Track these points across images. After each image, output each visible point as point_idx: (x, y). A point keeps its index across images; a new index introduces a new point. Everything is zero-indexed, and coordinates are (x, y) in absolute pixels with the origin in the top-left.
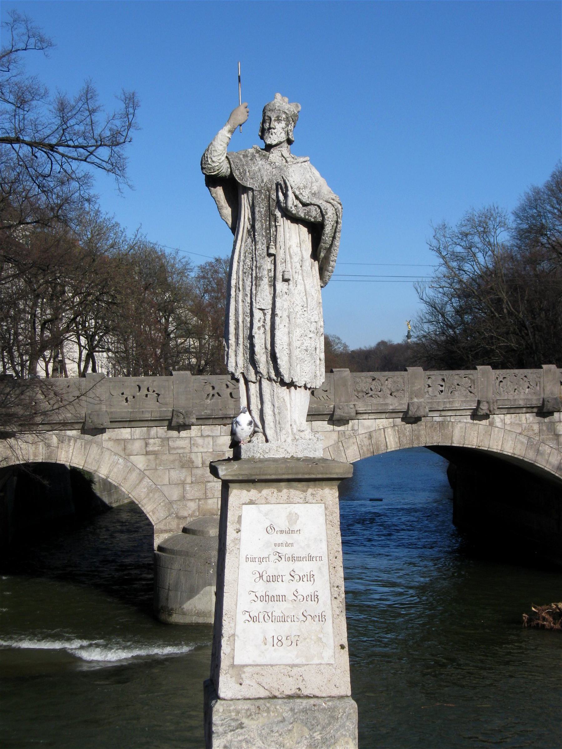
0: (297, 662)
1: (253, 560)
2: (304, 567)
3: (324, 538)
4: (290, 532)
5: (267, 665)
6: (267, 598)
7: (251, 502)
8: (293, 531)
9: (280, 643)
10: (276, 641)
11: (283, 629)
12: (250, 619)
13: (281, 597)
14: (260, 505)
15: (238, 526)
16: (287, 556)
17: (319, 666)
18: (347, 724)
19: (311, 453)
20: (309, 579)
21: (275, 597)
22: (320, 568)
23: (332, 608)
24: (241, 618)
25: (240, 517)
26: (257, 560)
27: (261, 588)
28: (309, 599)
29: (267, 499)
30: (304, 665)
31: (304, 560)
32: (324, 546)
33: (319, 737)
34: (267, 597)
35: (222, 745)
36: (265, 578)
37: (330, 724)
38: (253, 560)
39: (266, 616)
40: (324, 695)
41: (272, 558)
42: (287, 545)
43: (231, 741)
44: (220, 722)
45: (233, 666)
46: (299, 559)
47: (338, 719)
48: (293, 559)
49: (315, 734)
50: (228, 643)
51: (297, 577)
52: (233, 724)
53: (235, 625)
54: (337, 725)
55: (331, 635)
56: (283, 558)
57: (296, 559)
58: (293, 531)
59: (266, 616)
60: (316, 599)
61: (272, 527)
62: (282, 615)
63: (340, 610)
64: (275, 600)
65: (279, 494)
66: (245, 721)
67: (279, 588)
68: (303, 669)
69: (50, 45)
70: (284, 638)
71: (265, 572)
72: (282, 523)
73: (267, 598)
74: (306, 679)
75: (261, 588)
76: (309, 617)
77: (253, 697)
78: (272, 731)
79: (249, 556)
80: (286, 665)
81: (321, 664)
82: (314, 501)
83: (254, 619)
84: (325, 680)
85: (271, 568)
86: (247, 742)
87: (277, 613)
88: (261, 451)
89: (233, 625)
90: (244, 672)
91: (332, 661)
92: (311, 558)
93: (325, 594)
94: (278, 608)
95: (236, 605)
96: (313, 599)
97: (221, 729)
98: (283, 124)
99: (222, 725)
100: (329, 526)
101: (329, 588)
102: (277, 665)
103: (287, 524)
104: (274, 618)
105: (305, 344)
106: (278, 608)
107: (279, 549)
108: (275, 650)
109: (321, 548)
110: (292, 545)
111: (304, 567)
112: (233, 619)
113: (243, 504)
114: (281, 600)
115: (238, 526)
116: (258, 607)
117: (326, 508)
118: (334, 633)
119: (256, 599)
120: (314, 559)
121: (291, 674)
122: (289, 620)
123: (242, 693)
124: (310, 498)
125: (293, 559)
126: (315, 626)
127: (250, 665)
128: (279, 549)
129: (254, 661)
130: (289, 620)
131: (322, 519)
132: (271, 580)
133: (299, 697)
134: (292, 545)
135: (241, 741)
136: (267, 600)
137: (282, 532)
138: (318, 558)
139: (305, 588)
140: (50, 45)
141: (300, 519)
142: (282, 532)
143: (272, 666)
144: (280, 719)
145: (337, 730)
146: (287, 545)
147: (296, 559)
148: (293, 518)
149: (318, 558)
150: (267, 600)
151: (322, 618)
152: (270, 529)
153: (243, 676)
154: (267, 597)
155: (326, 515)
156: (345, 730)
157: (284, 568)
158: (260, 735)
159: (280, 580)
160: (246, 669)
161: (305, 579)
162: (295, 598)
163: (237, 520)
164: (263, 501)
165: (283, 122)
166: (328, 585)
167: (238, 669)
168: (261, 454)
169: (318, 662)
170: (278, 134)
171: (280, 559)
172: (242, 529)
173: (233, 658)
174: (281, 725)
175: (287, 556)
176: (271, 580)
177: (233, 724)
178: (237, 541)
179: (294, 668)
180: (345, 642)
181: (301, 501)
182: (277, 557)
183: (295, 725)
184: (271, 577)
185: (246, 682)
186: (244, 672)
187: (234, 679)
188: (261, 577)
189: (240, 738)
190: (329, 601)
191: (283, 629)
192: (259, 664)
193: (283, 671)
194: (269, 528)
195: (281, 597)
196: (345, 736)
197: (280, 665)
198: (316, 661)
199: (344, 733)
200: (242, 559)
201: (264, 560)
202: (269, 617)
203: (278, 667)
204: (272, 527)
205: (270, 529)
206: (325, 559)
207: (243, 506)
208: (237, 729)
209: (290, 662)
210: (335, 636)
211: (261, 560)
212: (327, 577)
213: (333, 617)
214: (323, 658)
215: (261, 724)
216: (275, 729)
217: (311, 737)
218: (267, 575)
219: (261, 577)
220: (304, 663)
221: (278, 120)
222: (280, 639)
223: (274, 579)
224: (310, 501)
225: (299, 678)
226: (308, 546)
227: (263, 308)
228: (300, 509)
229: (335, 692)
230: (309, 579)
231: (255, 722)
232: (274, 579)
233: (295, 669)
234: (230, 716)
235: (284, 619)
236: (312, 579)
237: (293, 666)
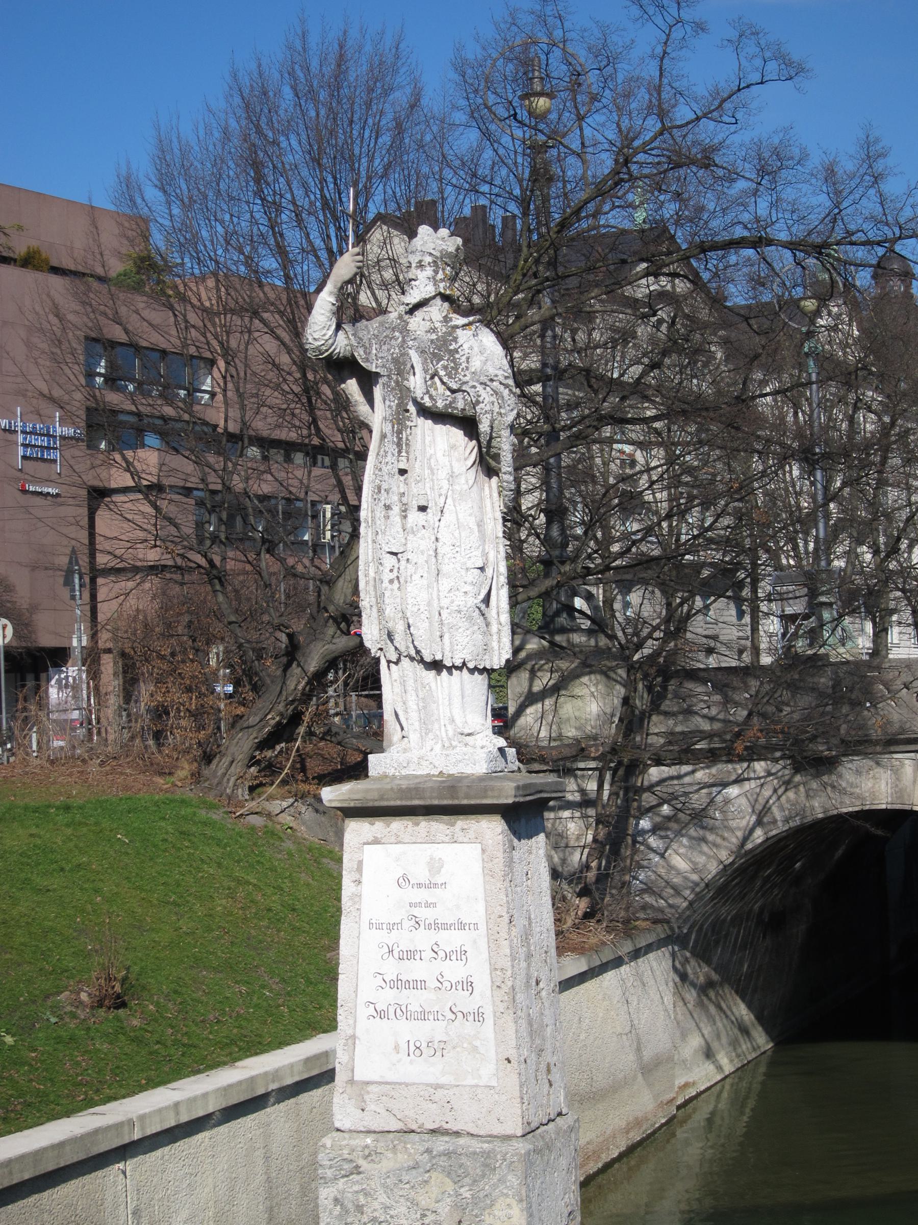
0: (443, 1080)
1: (379, 927)
2: (451, 940)
3: (480, 894)
4: (432, 885)
5: (400, 1084)
6: (398, 984)
7: (376, 841)
9: (418, 1052)
10: (412, 1048)
11: (422, 1031)
15: (358, 876)
18: (509, 1178)
22: (475, 942)
23: (494, 1002)
24: (364, 1012)
25: (360, 863)
27: (391, 969)
28: (460, 987)
29: (398, 836)
32: (481, 907)
33: (468, 1195)
35: (332, 1195)
36: (396, 953)
37: (483, 1176)
38: (379, 927)
39: (398, 1011)
41: (407, 924)
42: (428, 905)
43: (344, 1192)
44: (328, 1163)
45: (351, 1082)
46: (446, 927)
47: (495, 1169)
48: (437, 926)
49: (462, 1190)
52: (346, 1166)
54: (495, 1179)
56: (422, 924)
59: (398, 1011)
61: (405, 877)
63: (505, 1004)
65: (416, 828)
66: (361, 1162)
67: (416, 970)
68: (451, 1092)
69: (801, 70)
70: (424, 1045)
72: (421, 874)
73: (398, 984)
74: (455, 1107)
75: (391, 969)
76: (460, 1015)
77: (381, 1129)
78: (400, 1181)
80: (427, 1085)
81: (477, 1086)
82: (465, 840)
83: (381, 1014)
84: (484, 1110)
85: (405, 939)
86: (366, 1194)
87: (414, 1007)
88: (395, 765)
89: (351, 1022)
90: (368, 1093)
91: (494, 1083)
92: (462, 926)
93: (483, 981)
94: (415, 1000)
95: (356, 992)
97: (329, 1173)
98: (429, 271)
99: (331, 1167)
100: (488, 878)
103: (427, 873)
105: (457, 603)
106: (415, 1000)
107: (416, 911)
108: (411, 1062)
111: (451, 940)
112: (353, 1014)
113: (365, 844)
115: (358, 876)
116: (385, 998)
117: (483, 851)
118: (496, 1038)
119: (384, 985)
121: (435, 1098)
122: (431, 1017)
124: (459, 835)
125: (437, 926)
126: (469, 1027)
127: (376, 1083)
128: (416, 911)
130: (431, 1017)
131: (477, 867)
135: (357, 1192)
137: (419, 885)
139: (454, 971)
140: (801, 70)
142: (419, 885)
143: (407, 1085)
144: (411, 1163)
145: (495, 1186)
146: (428, 905)
148: (435, 866)
151: (479, 1016)
152: (404, 880)
153: (366, 1097)
156: (507, 1187)
157: (423, 940)
158: (384, 1186)
159: (417, 957)
160: (371, 1088)
161: (453, 957)
162: (439, 985)
164: (393, 839)
165: (428, 268)
166: (487, 967)
167: (360, 1087)
170: (422, 286)
172: (364, 879)
173: (353, 1071)
174: (414, 1172)
177: (346, 1166)
178: (357, 897)
180: (512, 1053)
181: (447, 839)
182: (413, 922)
183: (434, 1175)
185: (371, 1107)
186: (368, 1093)
187: (353, 1101)
188: (391, 951)
189: (356, 1188)
190: (489, 993)
191: (422, 1031)
193: (422, 1093)
194: (401, 880)
196: (507, 1195)
198: (470, 1081)
199: (505, 1191)
200: (365, 925)
202: (403, 1012)
204: (405, 877)
205: (404, 880)
206: (483, 927)
208: (352, 1174)
209: (432, 1080)
211: (391, 927)
212: (485, 955)
214: (480, 1077)
215: (385, 1170)
216: (405, 1178)
217: (458, 1195)
219: (391, 951)
220: (453, 1083)
221: (420, 265)
223: (410, 955)
224: (460, 839)
227: (395, 551)
228: (444, 851)
229: (498, 1130)
231: (376, 1166)
232: (410, 955)
233: (440, 1093)
234: (340, 1155)
235: (423, 1016)
237: (437, 1087)
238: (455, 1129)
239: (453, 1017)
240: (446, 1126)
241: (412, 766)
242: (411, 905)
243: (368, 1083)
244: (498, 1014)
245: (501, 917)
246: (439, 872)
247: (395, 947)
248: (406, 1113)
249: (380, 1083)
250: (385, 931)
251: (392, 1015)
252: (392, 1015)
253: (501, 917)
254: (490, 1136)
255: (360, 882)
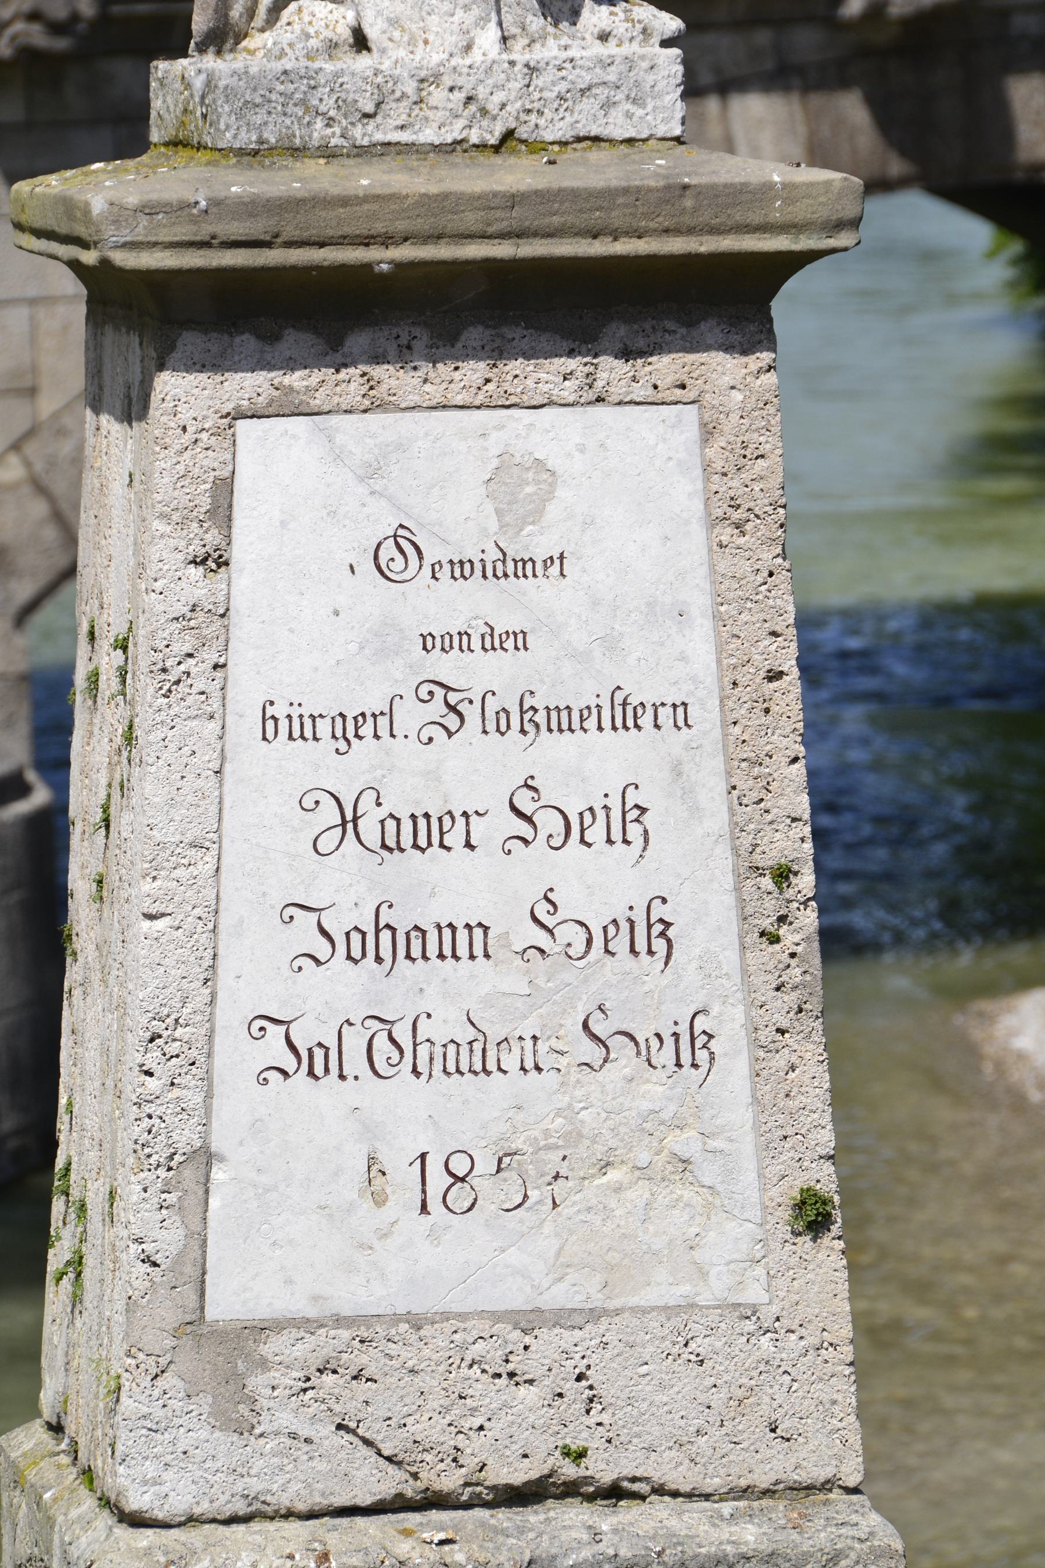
8: (524, 567)
10: (438, 1181)
12: (289, 1062)
13: (462, 935)
14: (334, 420)
15: (213, 537)
16: (493, 705)
17: (677, 1322)
19: (617, 115)
20: (617, 835)
21: (432, 937)
22: (677, 771)
23: (750, 990)
26: (324, 728)
28: (620, 944)
30: (595, 1315)
31: (591, 723)
34: (386, 936)
39: (381, 1043)
40: (712, 1483)
50: (172, 1198)
51: (549, 823)
53: (209, 1096)
55: (747, 1146)
56: (472, 713)
57: (541, 718)
58: (524, 567)
59: (381, 1043)
60: (659, 945)
62: (471, 1033)
63: (791, 999)
64: (432, 950)
70: (485, 1165)
71: (369, 797)
77: (319, 1501)
79: (279, 710)
80: (497, 1317)
84: (717, 1399)
88: (328, 105)
90: (264, 1364)
91: (754, 1294)
96: (641, 945)
100: (726, 533)
101: (729, 881)
102: (446, 1316)
103: (493, 525)
104: (423, 1051)
109: (683, 658)
110: (520, 640)
114: (463, 950)
117: (708, 432)
118: (756, 1126)
119: (322, 948)
120: (646, 721)
122: (510, 1062)
123: (255, 1485)
129: (316, 1298)
132: (407, 841)
133: (571, 1490)
134: (520, 640)
136: (386, 952)
138: (665, 713)
141: (560, 492)
143: (417, 1323)
147: (541, 718)
149: (665, 713)
150: (386, 952)
153: (258, 1383)
154: (386, 936)
155: (707, 467)
159: (455, 838)
160: (272, 1347)
161: (596, 833)
162: (541, 938)
163: (205, 502)
166: (723, 863)
168: (330, 122)
169: (675, 1294)
171: (453, 721)
172: (237, 554)
175: (493, 705)
176: (407, 841)
179: (543, 1333)
182: (437, 708)
184: (407, 827)
186: (264, 1364)
190: (731, 957)
192: (346, 1311)
194: (388, 550)
195: (462, 935)
197: (463, 1317)
201: (367, 730)
203: (448, 1326)
207: (241, 425)
210: (766, 1150)
213: (756, 1043)
214: (704, 1274)
218: (382, 812)
220: (598, 1300)
222: (460, 1166)
224: (617, 391)
225: (570, 1387)
226: (611, 643)
230: (617, 835)
236: (634, 832)
238: (607, 1478)
239: (593, 1053)
240: (569, 1471)
241: (398, 112)
242: (426, 642)
243: (262, 1329)
244: (767, 1035)
245: (775, 676)
246: (537, 514)
247: (367, 801)
248: (417, 1429)
249: (308, 1325)
250: (327, 744)
251: (355, 1062)
252: (355, 1062)
253: (775, 676)
254: (745, 1492)
255: (223, 563)
